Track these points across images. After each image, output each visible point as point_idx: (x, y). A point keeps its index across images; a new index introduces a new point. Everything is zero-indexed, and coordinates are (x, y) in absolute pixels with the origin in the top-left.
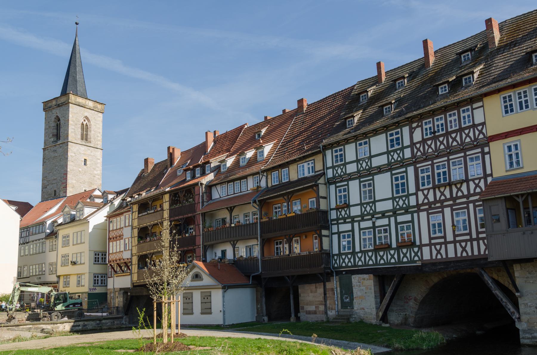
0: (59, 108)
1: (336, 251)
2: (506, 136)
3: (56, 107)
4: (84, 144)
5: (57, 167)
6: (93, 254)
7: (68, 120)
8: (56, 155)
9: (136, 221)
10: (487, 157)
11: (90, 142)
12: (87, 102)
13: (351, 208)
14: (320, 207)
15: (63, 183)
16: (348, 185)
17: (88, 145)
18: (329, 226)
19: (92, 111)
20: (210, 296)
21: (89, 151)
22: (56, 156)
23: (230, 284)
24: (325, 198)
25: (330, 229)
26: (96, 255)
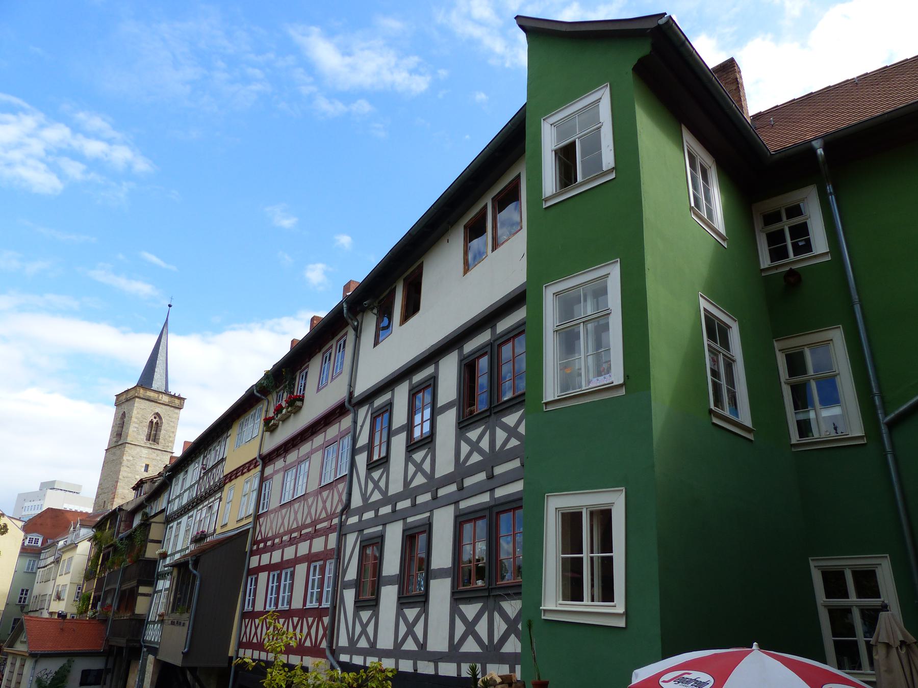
0: (127, 403)
1: (151, 618)
2: (231, 477)
3: (126, 401)
4: (149, 446)
6: (75, 588)
7: (132, 417)
8: (114, 458)
9: (93, 549)
11: (158, 444)
12: (161, 396)
13: (167, 558)
14: (144, 555)
15: (112, 494)
16: (172, 527)
18: (154, 581)
19: (166, 407)
20: (24, 665)
21: (155, 455)
22: (114, 460)
23: (48, 651)
24: (159, 542)
25: (155, 584)
26: (79, 589)
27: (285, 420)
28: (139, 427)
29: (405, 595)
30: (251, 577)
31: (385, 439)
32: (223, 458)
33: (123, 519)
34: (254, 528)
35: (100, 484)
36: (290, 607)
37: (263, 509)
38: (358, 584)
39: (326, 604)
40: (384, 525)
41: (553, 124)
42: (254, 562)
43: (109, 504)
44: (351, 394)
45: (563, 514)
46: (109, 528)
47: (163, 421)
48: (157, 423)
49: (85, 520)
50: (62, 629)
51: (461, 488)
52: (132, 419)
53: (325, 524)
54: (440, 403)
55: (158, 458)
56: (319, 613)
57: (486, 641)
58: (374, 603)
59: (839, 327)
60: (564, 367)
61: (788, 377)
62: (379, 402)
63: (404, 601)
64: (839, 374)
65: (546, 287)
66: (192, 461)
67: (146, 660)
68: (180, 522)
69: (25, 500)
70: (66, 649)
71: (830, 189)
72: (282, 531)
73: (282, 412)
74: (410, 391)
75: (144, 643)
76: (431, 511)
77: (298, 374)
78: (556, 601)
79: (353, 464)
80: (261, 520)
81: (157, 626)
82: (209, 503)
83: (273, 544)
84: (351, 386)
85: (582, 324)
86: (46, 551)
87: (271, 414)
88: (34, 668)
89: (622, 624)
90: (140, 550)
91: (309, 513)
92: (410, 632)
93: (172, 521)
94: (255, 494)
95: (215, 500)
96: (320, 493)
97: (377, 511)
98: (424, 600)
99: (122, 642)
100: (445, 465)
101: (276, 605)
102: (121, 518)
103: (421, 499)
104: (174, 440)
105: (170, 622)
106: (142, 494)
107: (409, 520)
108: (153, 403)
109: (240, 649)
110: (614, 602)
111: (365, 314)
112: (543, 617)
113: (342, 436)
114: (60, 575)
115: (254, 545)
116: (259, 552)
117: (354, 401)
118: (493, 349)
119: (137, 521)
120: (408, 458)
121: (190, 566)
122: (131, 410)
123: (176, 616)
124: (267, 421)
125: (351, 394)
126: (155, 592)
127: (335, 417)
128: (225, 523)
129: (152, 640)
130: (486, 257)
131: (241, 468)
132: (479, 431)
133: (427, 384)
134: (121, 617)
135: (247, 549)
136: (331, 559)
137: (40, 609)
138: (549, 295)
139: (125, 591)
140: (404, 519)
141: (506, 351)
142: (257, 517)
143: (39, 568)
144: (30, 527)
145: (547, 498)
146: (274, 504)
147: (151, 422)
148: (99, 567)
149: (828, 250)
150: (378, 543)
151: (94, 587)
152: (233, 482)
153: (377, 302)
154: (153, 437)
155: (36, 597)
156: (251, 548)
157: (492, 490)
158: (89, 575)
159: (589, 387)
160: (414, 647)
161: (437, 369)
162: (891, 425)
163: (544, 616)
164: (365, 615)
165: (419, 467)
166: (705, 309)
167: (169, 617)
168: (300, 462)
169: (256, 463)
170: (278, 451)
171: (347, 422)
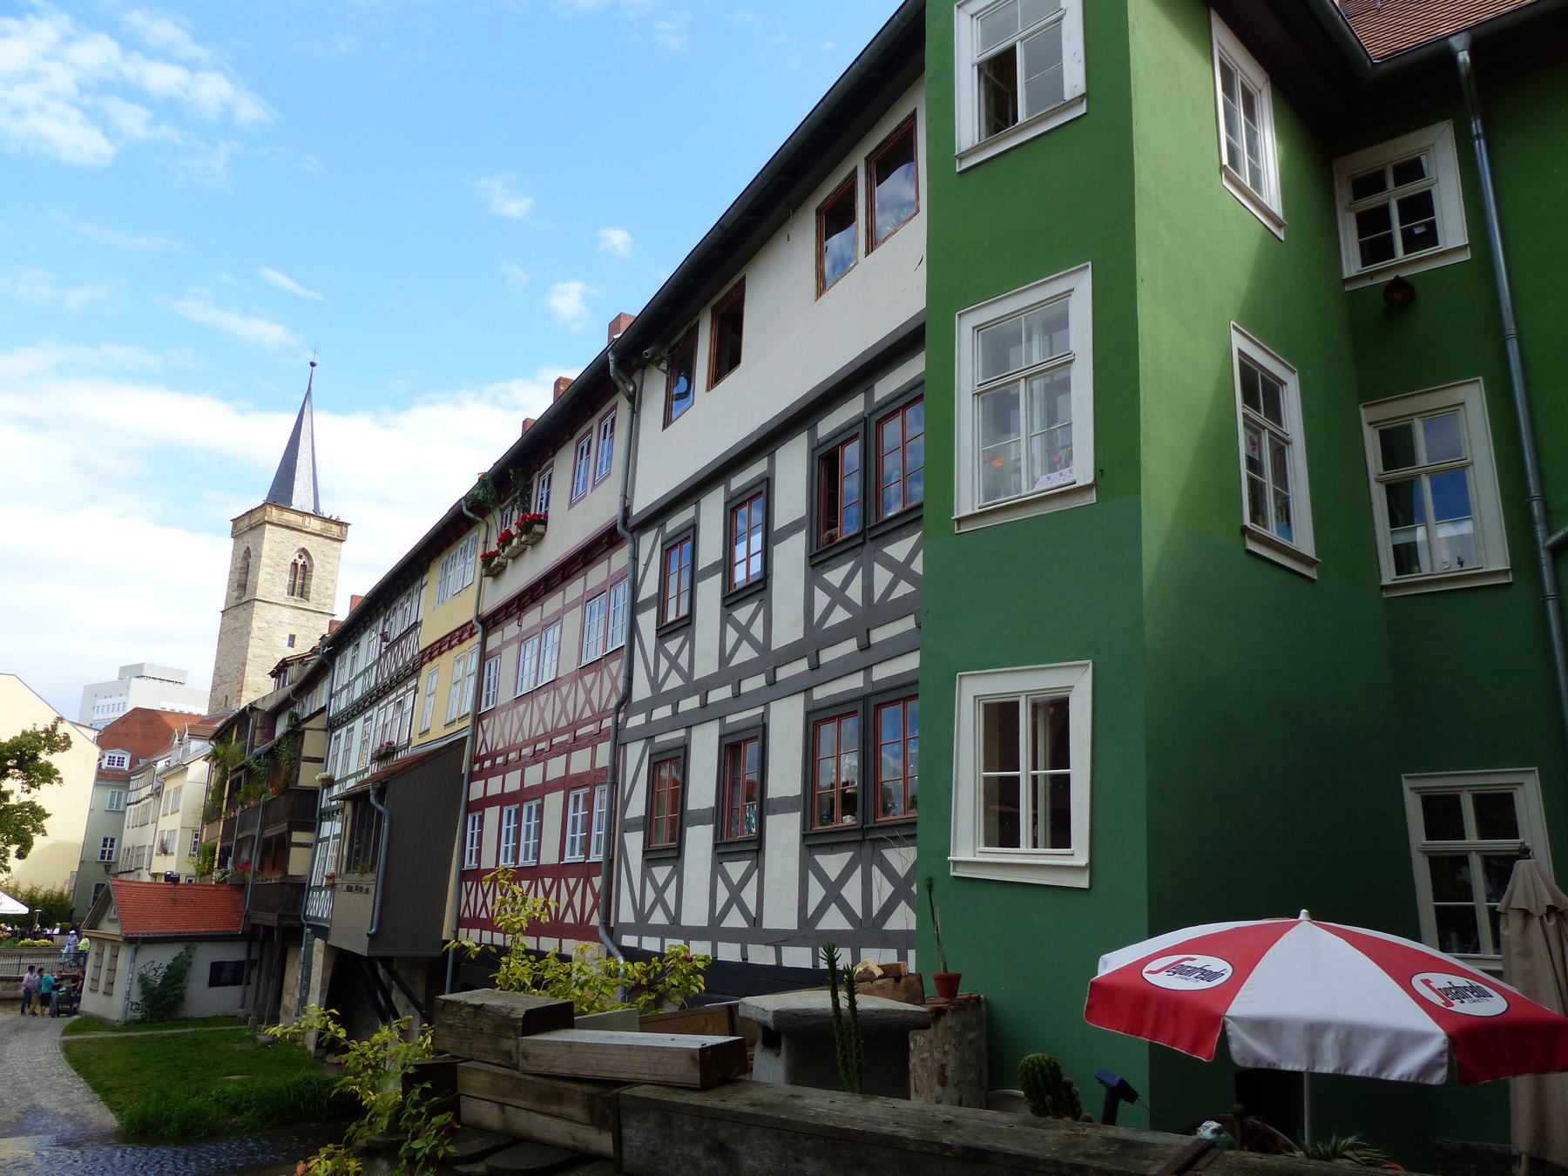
0: (252, 532)
1: (315, 881)
2: (431, 653)
4: (293, 604)
5: (234, 650)
6: (189, 836)
9: (214, 774)
10: (417, 695)
11: (308, 600)
12: (307, 519)
13: (335, 787)
14: (297, 781)
17: (301, 606)
19: (318, 538)
20: (117, 956)
21: (304, 619)
24: (320, 760)
26: (196, 836)
27: (516, 556)
28: (275, 573)
29: (725, 840)
30: (473, 814)
31: (685, 586)
32: (416, 623)
33: (258, 725)
34: (474, 736)
35: (217, 669)
36: (538, 862)
37: (487, 705)
38: (648, 824)
39: (595, 857)
40: (689, 728)
41: (976, 14)
42: (476, 790)
43: (234, 701)
44: (626, 511)
45: (986, 705)
46: (237, 739)
47: (315, 562)
48: (304, 566)
49: (196, 726)
50: (174, 900)
51: (815, 666)
52: (262, 559)
53: (591, 728)
54: (779, 522)
55: (310, 624)
56: (585, 871)
57: (859, 912)
58: (674, 854)
59: (1478, 381)
60: (990, 457)
61: (1381, 471)
62: (674, 523)
63: (724, 849)
64: (1472, 463)
65: (960, 316)
66: (366, 628)
67: (312, 946)
68: (352, 729)
69: (96, 696)
70: (181, 930)
71: (1476, 127)
72: (520, 739)
73: (511, 542)
74: (726, 503)
75: (306, 920)
76: (766, 704)
77: (535, 477)
78: (975, 848)
79: (633, 629)
80: (485, 722)
81: (326, 893)
82: (398, 697)
83: (507, 761)
84: (625, 497)
85: (1023, 380)
86: (138, 777)
87: (493, 547)
88: (133, 960)
89: (1083, 882)
90: (290, 775)
91: (564, 710)
92: (735, 898)
93: (339, 726)
94: (472, 681)
95: (407, 691)
96: (581, 677)
97: (676, 706)
98: (756, 848)
99: (270, 919)
100: (788, 627)
101: (516, 858)
102: (255, 723)
103: (749, 685)
104: (334, 595)
105: (345, 887)
106: (287, 684)
107: (730, 719)
108: (296, 532)
109: (460, 929)
110: (1070, 848)
111: (646, 372)
112: (952, 874)
113: (614, 582)
114: (163, 816)
115: (475, 763)
116: (484, 775)
117: (631, 523)
118: (868, 429)
119: (281, 727)
120: (726, 618)
121: (372, 799)
122: (259, 545)
123: (354, 878)
124: (487, 558)
125: (626, 511)
126: (318, 840)
127: (602, 550)
128: (426, 728)
129: (319, 916)
130: (855, 265)
131: (448, 638)
132: (845, 569)
133: (756, 490)
134: (267, 880)
135: (465, 769)
136: (602, 783)
137: (136, 869)
138: (966, 329)
139: (269, 839)
140: (722, 718)
141: (892, 431)
142: (478, 718)
143: (129, 804)
144: (109, 738)
145: (960, 680)
146: (505, 695)
147: (295, 564)
148: (225, 801)
149: (1467, 242)
150: (679, 757)
151: (220, 833)
152: (436, 661)
153: (666, 350)
154: (300, 590)
155: (129, 850)
156: (471, 768)
157: (867, 668)
158: (210, 815)
159: (1034, 490)
160: (742, 923)
161: (772, 464)
162: (1557, 551)
163: (954, 870)
164: (661, 873)
165: (744, 632)
166: (1241, 352)
167: (343, 879)
168: (545, 626)
169: (472, 629)
170: (507, 609)
171: (620, 558)
